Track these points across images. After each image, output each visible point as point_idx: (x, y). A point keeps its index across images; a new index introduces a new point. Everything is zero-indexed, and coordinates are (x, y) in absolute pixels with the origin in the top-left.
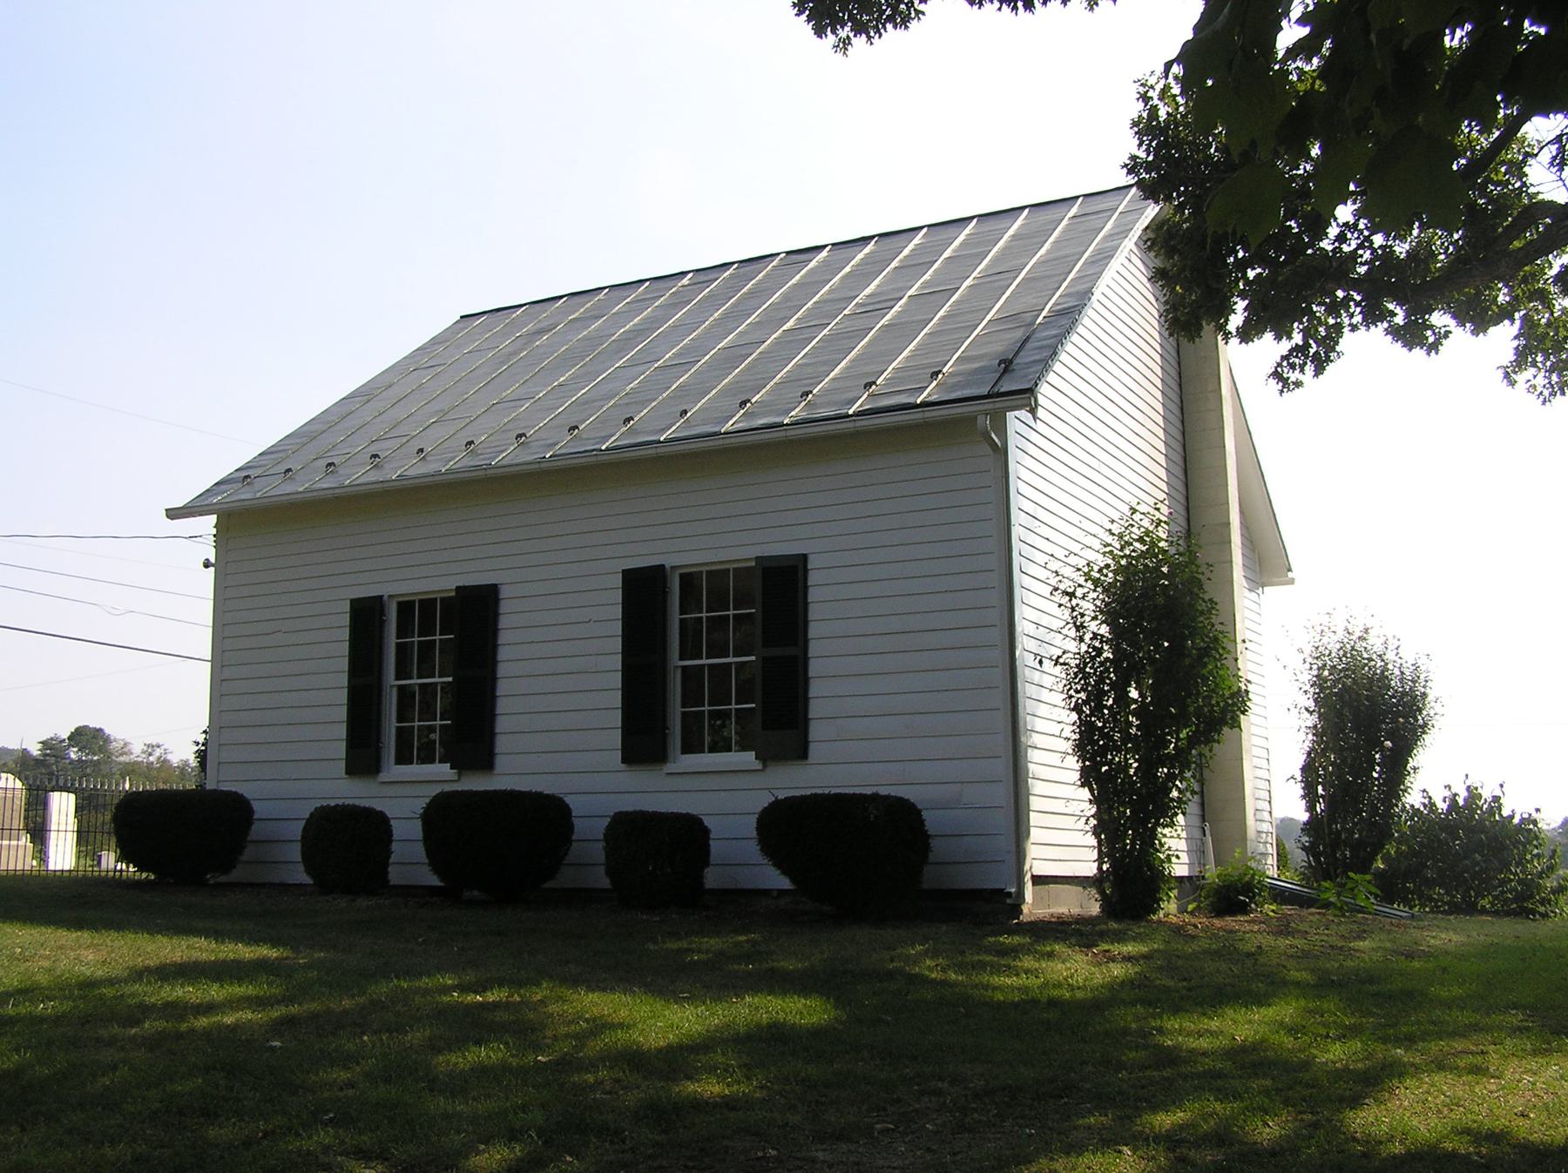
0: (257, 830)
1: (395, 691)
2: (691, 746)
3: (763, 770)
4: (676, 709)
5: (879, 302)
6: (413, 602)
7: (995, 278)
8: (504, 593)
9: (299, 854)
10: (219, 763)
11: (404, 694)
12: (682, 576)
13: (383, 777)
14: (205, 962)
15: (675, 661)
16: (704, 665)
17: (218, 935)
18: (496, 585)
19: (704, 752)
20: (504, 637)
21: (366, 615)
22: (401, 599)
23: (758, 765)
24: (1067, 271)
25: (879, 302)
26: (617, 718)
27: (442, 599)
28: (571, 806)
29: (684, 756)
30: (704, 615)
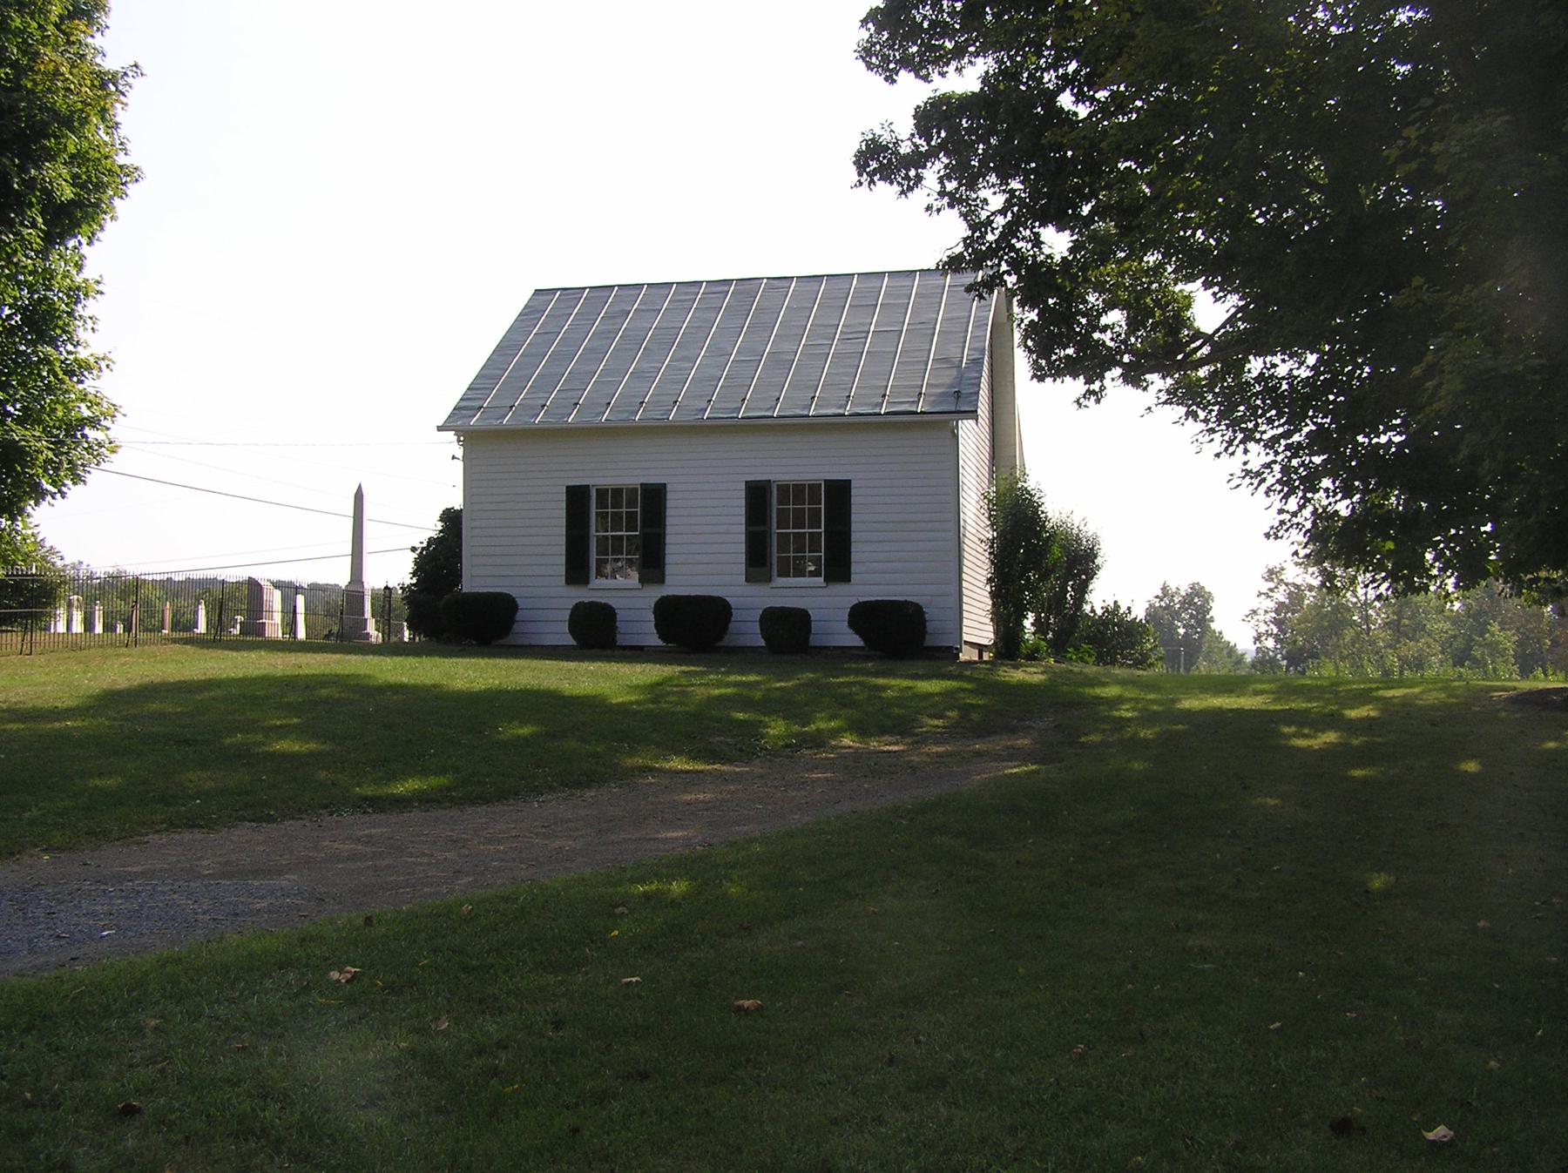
0: (520, 615)
1: (595, 539)
2: (784, 573)
3: (825, 587)
4: (593, 557)
5: (851, 333)
6: (607, 490)
7: (919, 326)
8: (669, 488)
9: (567, 628)
10: (472, 576)
11: (602, 542)
12: (778, 485)
13: (590, 586)
14: (749, 674)
15: (775, 530)
16: (790, 533)
17: (686, 665)
18: (665, 484)
19: (790, 576)
20: (669, 512)
21: (577, 497)
22: (599, 487)
23: (825, 585)
24: (964, 329)
25: (851, 333)
26: (563, 560)
27: (612, 489)
28: (920, 604)
29: (779, 578)
30: (807, 506)
